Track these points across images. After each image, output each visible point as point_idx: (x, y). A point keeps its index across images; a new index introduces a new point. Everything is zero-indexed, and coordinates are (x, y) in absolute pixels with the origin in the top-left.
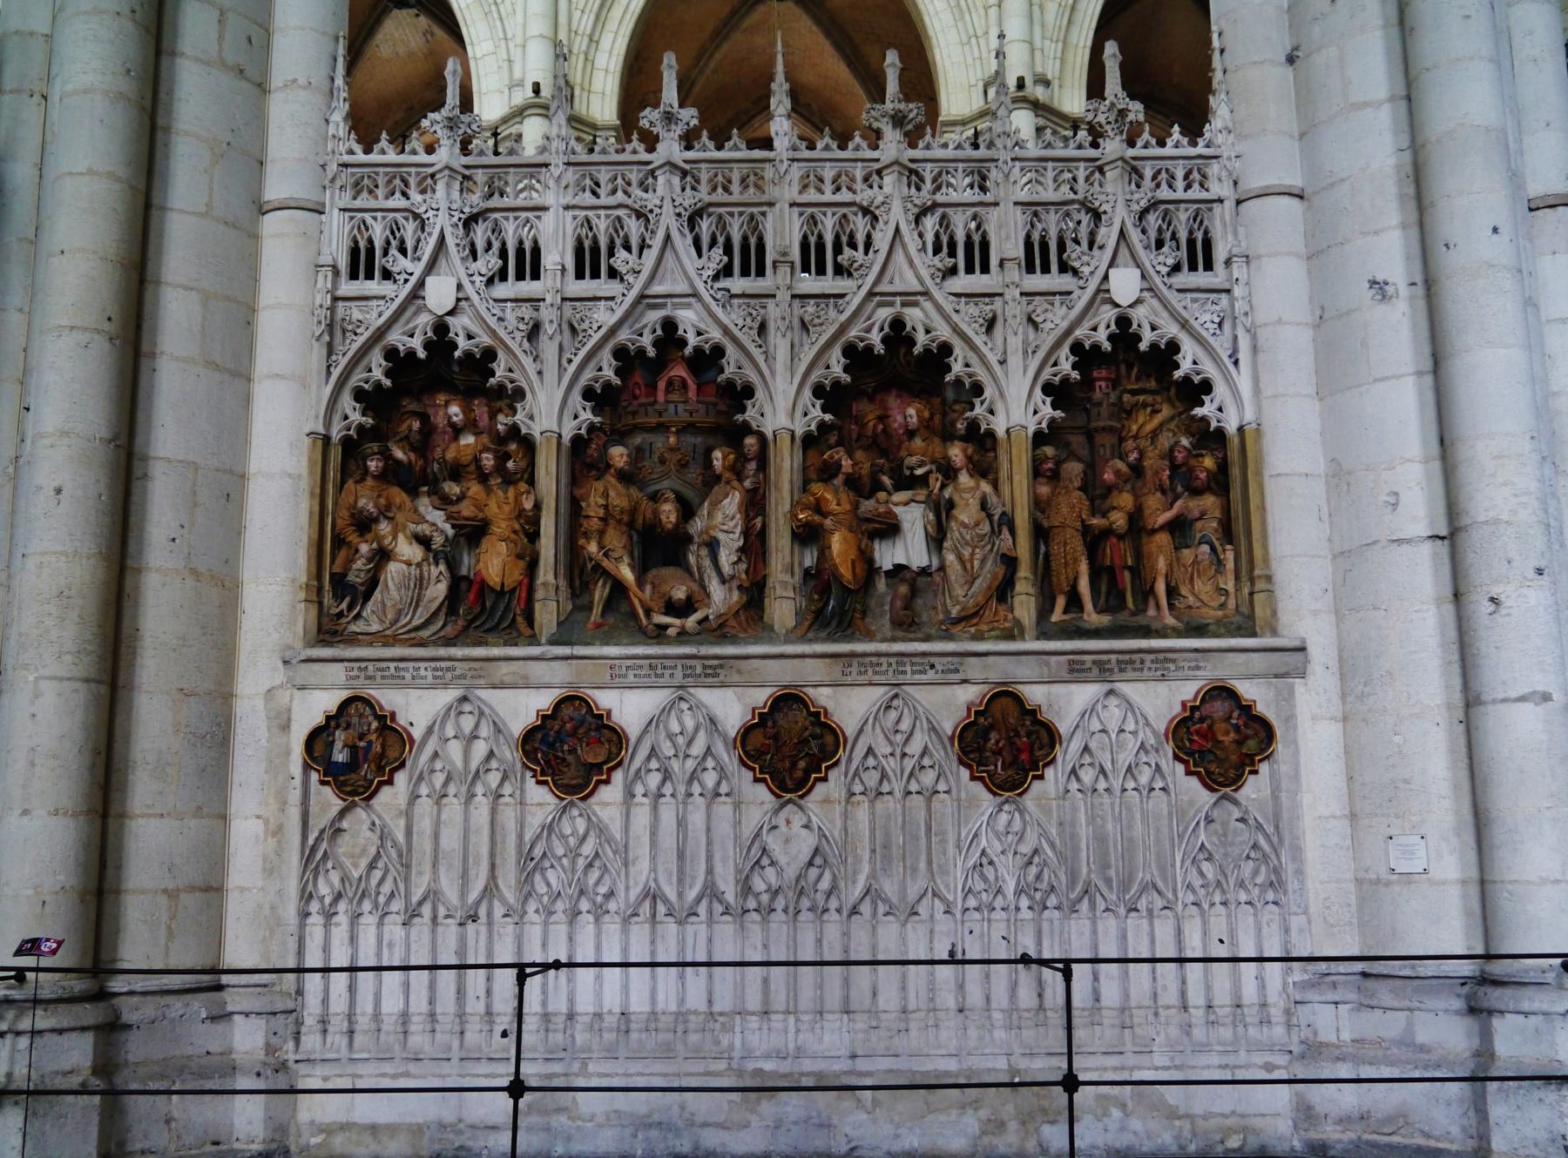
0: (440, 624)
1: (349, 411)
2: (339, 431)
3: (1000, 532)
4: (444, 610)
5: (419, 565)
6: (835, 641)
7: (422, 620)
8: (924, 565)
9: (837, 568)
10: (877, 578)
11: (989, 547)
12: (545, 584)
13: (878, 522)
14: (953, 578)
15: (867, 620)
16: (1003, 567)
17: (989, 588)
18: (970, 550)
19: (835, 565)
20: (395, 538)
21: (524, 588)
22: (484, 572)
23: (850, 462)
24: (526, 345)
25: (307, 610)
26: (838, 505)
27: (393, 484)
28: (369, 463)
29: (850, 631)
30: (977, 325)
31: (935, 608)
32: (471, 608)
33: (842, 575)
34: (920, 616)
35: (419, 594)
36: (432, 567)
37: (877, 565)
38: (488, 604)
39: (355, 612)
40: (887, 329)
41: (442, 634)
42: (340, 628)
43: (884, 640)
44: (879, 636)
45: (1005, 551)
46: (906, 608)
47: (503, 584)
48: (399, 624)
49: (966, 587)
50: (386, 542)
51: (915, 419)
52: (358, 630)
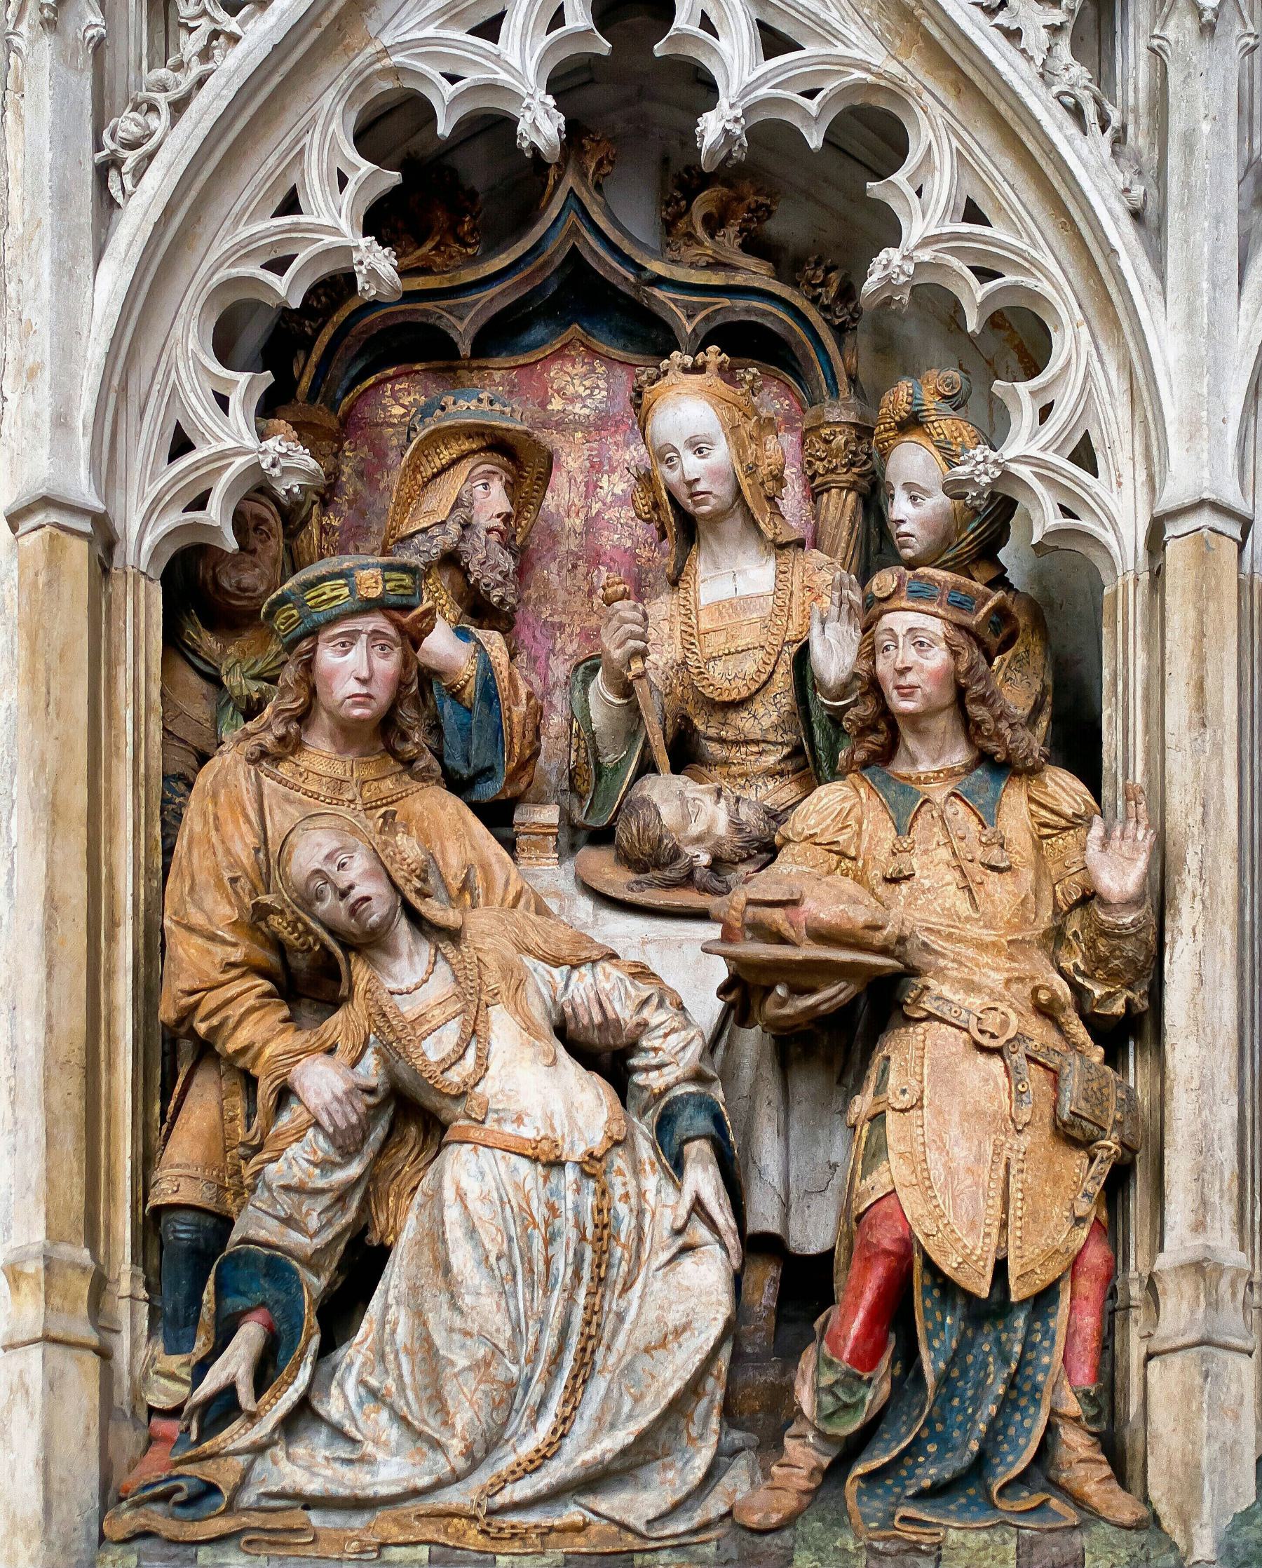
0: (702, 1460)
1: (201, 410)
2: (156, 508)
4: (715, 1389)
5: (592, 1166)
7: (623, 1437)
12: (1200, 1268)
20: (474, 1033)
21: (1088, 1287)
22: (912, 1205)
24: (1076, 74)
25: (52, 1384)
27: (423, 777)
28: (327, 657)
32: (852, 1381)
35: (592, 1311)
36: (651, 1181)
38: (930, 1365)
39: (291, 1396)
41: (714, 1506)
42: (225, 1474)
47: (1001, 1268)
48: (506, 1461)
50: (435, 1048)
52: (313, 1487)
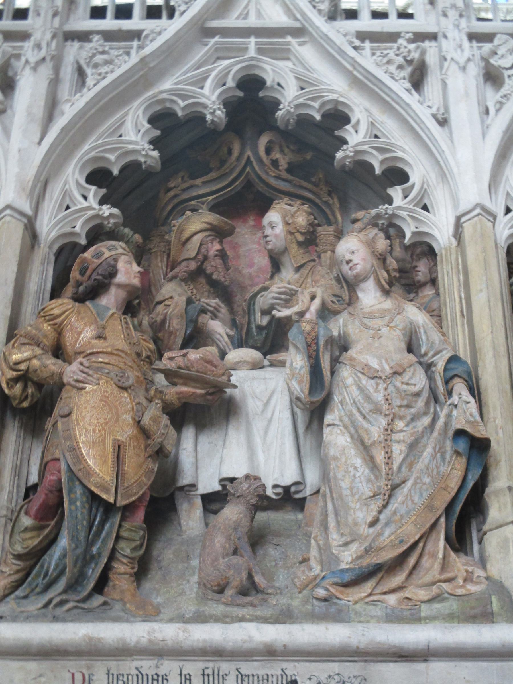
3: (450, 393)
6: (55, 619)
8: (287, 480)
9: (79, 458)
10: (183, 507)
11: (426, 420)
13: (187, 380)
14: (345, 485)
15: (147, 585)
16: (461, 464)
17: (429, 507)
18: (383, 422)
19: (75, 450)
23: (136, 268)
26: (99, 337)
29: (98, 600)
30: (392, 68)
31: (305, 560)
33: (88, 471)
34: (270, 577)
37: (185, 480)
40: (231, 83)
43: (182, 619)
44: (167, 612)
45: (458, 424)
46: (235, 552)
49: (375, 506)
51: (280, 229)
